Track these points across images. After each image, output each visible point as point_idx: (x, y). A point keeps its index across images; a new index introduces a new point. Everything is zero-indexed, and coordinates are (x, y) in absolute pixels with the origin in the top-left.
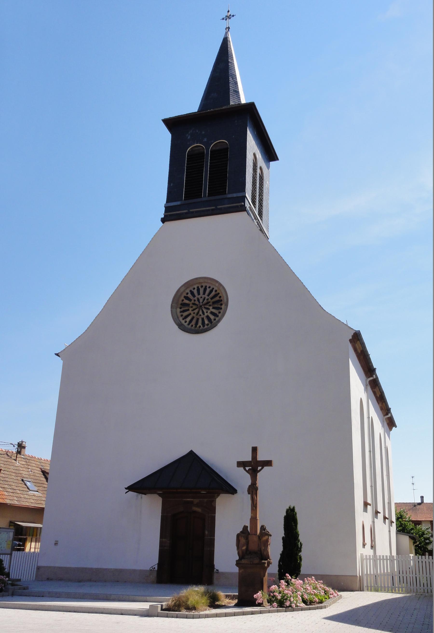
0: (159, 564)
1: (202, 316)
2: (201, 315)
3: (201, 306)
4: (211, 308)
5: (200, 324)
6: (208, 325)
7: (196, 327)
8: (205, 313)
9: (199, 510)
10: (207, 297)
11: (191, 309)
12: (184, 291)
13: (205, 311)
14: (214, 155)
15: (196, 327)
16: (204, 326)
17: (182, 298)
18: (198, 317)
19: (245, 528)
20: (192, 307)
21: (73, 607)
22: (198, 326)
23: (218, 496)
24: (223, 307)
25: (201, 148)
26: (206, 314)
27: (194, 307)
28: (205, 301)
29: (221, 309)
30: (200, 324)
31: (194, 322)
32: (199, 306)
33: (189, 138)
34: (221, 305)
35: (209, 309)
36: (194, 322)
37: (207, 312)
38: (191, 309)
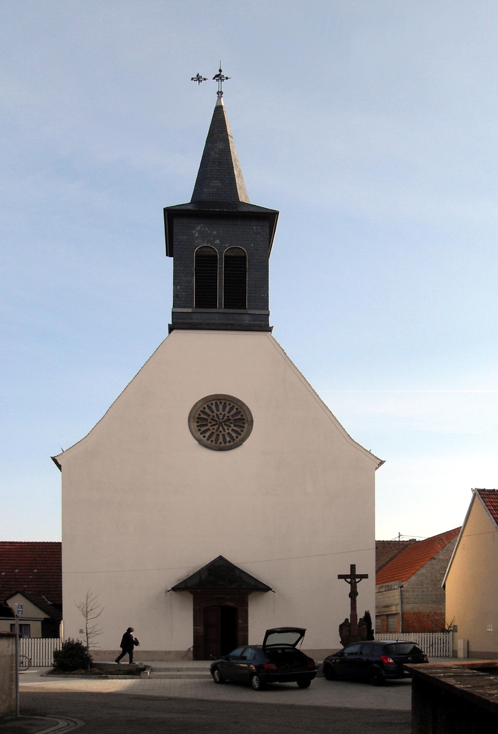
0: (194, 647)
1: (223, 433)
2: (221, 432)
3: (221, 423)
4: (232, 425)
5: (221, 439)
6: (229, 442)
7: (216, 442)
8: (226, 430)
9: (232, 604)
10: (227, 415)
11: (209, 425)
12: (201, 406)
13: (226, 428)
14: (221, 256)
15: (216, 442)
16: (225, 443)
17: (199, 412)
18: (218, 433)
19: (347, 620)
20: (210, 423)
21: (38, 688)
22: (219, 442)
23: (251, 592)
24: (246, 425)
25: (211, 250)
26: (227, 431)
27: (213, 423)
28: (226, 418)
29: (244, 427)
30: (221, 439)
31: (213, 438)
32: (221, 422)
33: (197, 235)
34: (244, 423)
35: (230, 426)
36: (213, 438)
37: (228, 429)
38: (209, 425)
